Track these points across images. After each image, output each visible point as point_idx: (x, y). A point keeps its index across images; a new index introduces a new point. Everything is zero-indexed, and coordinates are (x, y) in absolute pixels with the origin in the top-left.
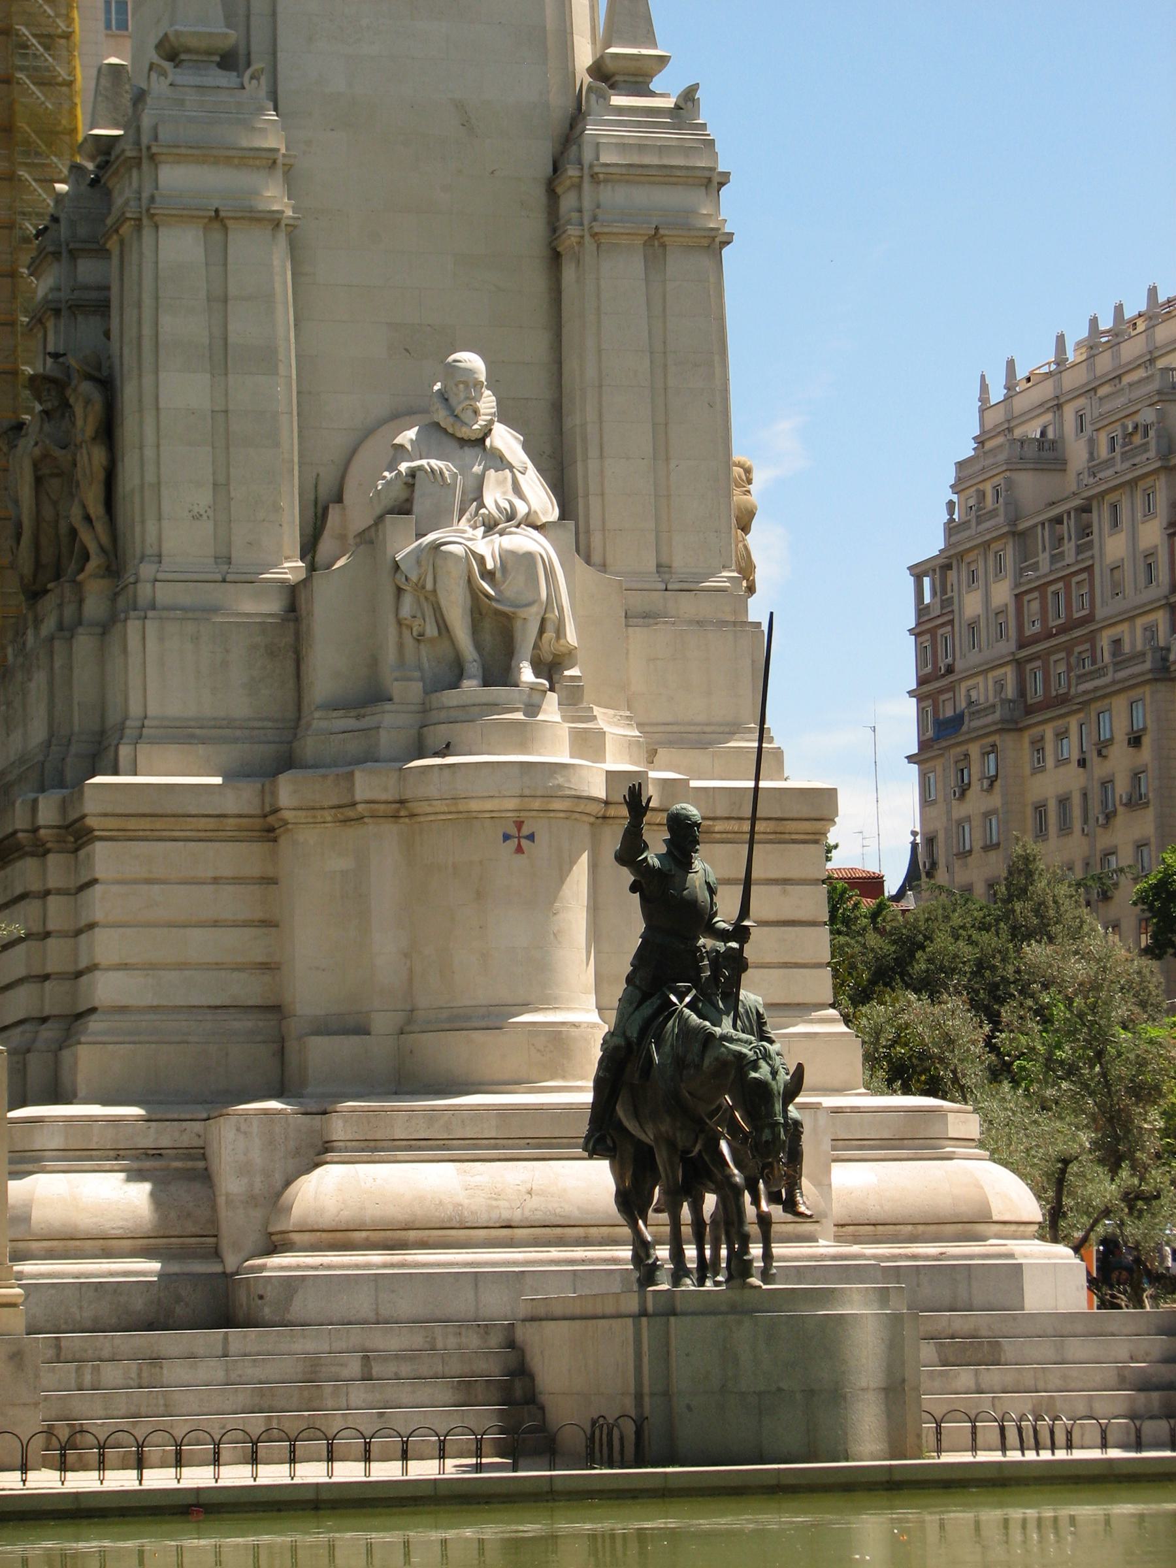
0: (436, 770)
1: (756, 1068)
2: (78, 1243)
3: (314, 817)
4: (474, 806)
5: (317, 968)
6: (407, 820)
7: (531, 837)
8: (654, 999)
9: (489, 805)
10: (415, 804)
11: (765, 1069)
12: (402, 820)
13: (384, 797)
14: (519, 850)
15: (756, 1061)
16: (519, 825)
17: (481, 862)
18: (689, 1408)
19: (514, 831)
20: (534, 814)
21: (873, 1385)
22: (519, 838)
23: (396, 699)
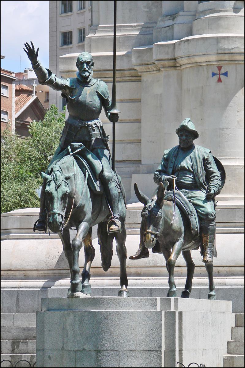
0: (183, 42)
1: (49, 185)
2: (13, 272)
3: (149, 69)
4: (198, 59)
5: (151, 142)
6: (179, 68)
7: (226, 74)
8: (64, 151)
9: (203, 59)
10: (180, 59)
11: (53, 184)
12: (178, 68)
13: (166, 57)
14: (220, 80)
15: (50, 181)
16: (220, 68)
17: (202, 87)
18: (50, 357)
19: (217, 71)
20: (226, 62)
21: (139, 349)
22: (220, 74)
23: (185, 9)
